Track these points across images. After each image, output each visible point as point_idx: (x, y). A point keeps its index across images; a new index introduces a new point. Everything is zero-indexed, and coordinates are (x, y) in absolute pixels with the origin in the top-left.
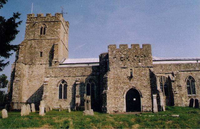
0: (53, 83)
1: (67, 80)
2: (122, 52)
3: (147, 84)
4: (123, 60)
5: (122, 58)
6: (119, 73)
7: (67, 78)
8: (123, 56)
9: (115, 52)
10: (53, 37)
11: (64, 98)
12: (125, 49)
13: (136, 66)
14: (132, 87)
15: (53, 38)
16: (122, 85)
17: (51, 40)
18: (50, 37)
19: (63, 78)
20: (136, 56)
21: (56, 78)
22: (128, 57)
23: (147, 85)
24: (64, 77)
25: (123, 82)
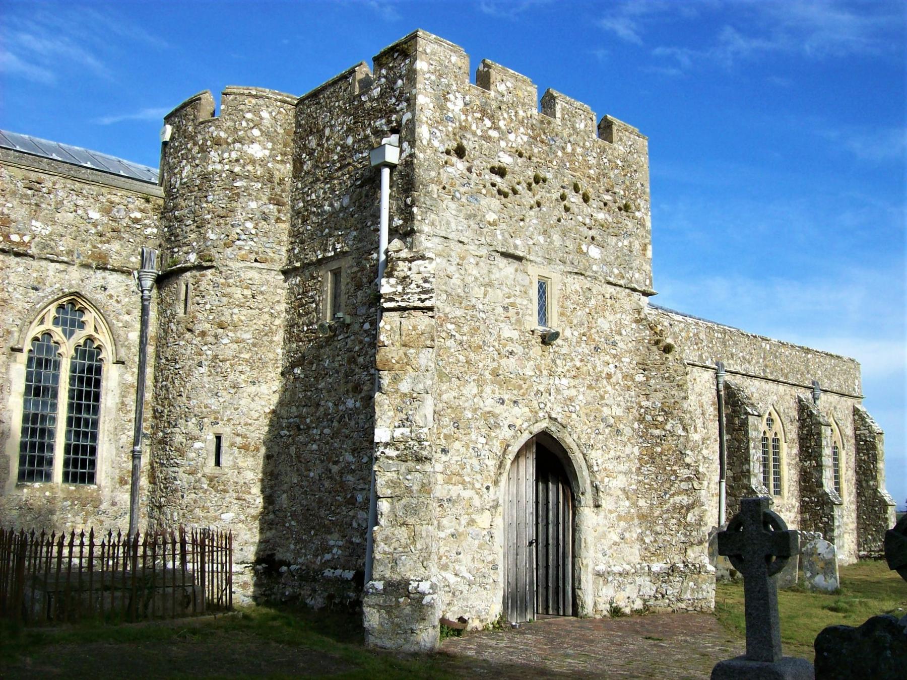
6: (478, 292)
8: (506, 160)
9: (460, 104)
16: (489, 404)
23: (618, 419)
25: (495, 373)
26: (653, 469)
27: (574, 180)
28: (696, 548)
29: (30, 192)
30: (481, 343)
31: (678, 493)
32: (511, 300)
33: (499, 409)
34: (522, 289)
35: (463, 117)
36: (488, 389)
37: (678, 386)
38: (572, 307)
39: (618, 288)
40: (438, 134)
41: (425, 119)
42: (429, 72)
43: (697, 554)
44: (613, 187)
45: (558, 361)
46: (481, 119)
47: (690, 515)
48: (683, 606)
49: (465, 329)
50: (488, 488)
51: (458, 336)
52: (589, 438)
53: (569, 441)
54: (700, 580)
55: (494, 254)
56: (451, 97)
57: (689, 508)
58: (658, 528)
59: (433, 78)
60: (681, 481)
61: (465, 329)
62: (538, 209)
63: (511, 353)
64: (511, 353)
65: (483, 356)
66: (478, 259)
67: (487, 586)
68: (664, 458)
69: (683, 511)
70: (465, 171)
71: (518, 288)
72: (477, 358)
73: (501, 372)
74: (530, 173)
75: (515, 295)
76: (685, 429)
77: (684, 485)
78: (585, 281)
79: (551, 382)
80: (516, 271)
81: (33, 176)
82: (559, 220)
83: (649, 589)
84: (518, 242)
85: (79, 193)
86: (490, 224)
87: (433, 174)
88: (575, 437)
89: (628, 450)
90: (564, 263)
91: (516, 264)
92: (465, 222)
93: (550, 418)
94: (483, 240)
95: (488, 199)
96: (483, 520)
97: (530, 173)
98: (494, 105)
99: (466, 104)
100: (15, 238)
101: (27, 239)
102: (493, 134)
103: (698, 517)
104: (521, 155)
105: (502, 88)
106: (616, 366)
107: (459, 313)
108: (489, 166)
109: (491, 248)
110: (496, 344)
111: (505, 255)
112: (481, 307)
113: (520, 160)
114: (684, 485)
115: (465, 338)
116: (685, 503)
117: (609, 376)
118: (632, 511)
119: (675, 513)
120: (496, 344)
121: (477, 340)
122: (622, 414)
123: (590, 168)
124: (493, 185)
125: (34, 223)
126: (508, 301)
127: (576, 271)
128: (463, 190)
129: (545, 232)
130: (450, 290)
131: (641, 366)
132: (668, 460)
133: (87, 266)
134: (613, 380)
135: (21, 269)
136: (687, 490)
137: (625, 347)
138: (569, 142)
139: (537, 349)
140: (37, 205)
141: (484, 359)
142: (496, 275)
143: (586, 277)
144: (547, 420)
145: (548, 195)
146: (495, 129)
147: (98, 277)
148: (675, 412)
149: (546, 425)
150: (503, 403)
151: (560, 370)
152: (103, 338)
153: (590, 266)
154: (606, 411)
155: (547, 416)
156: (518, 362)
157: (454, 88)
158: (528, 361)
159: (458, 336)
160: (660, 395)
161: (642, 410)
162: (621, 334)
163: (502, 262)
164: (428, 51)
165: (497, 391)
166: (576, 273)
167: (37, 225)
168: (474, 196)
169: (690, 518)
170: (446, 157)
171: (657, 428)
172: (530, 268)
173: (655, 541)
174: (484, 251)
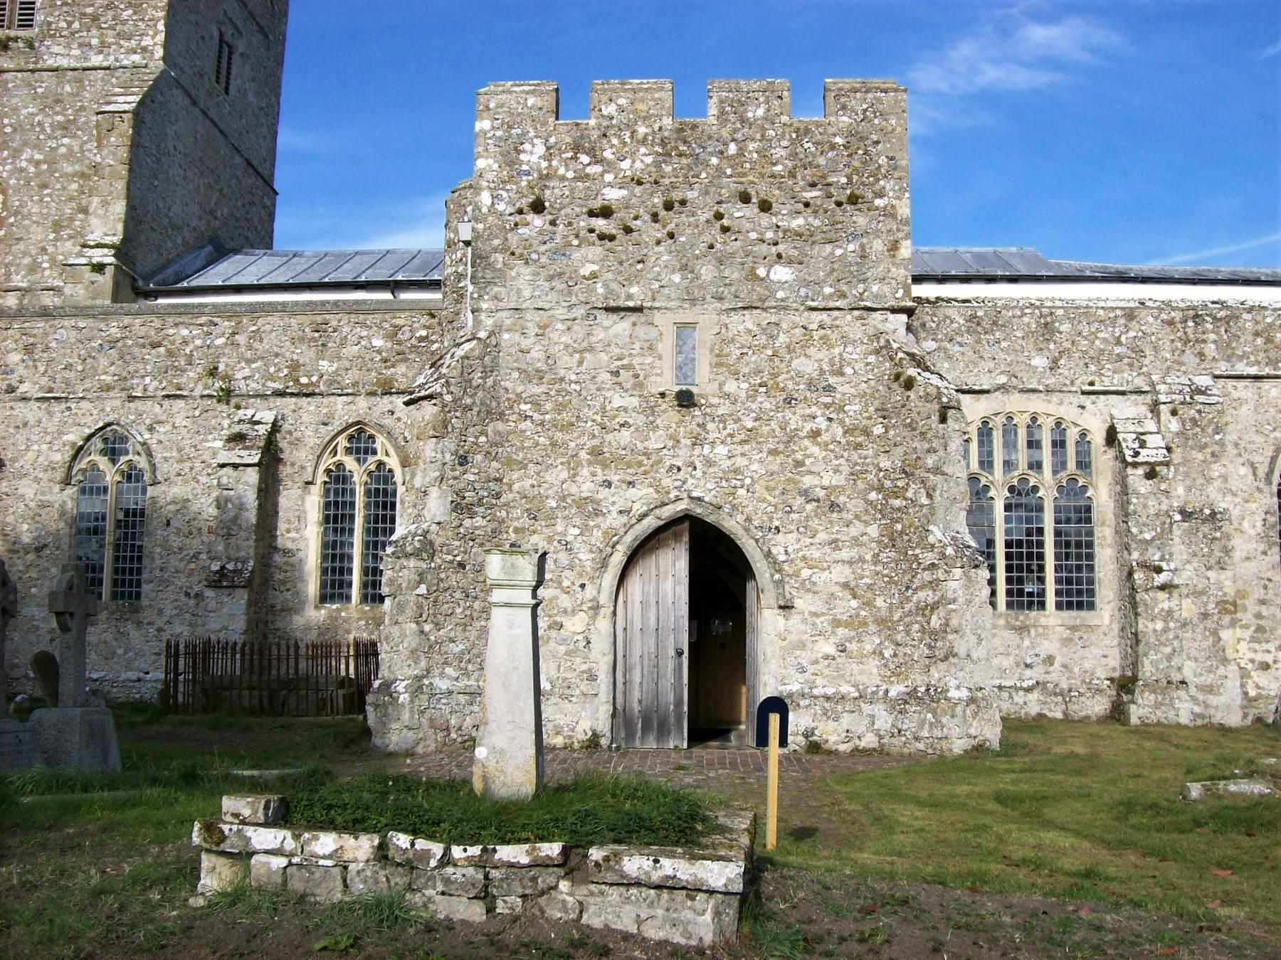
0: (31, 455)
1: (151, 429)
2: (608, 154)
3: (839, 480)
4: (612, 238)
5: (606, 212)
6: (568, 361)
7: (154, 409)
8: (613, 195)
9: (540, 149)
10: (103, 47)
11: (115, 596)
12: (642, 130)
13: (749, 293)
14: (681, 506)
15: (96, 60)
16: (586, 487)
17: (81, 81)
18: (76, 52)
19: (113, 409)
20: (745, 198)
21: (57, 408)
22: (668, 206)
24: (132, 398)
25: (596, 453)
26: (893, 554)
27: (741, 188)
28: (941, 666)
29: (317, 335)
30: (574, 419)
31: (922, 587)
32: (625, 362)
33: (603, 493)
34: (646, 345)
35: (544, 164)
36: (585, 472)
37: (922, 434)
38: (738, 352)
39: (836, 313)
40: (504, 194)
41: (485, 184)
42: (493, 128)
43: (942, 674)
44: (824, 177)
45: (710, 426)
46: (575, 158)
47: (934, 618)
48: (921, 746)
49: (548, 406)
50: (583, 586)
51: (536, 416)
52: (771, 519)
53: (731, 525)
54: (939, 711)
55: (595, 312)
56: (527, 147)
57: (934, 607)
58: (899, 638)
59: (499, 133)
60: (924, 570)
61: (548, 406)
62: (670, 241)
63: (622, 425)
64: (622, 425)
65: (575, 435)
66: (569, 323)
67: (574, 699)
68: (906, 538)
69: (927, 612)
70: (547, 226)
71: (637, 346)
72: (567, 437)
73: (605, 450)
74: (658, 200)
75: (630, 355)
76: (929, 496)
77: (927, 576)
78: (764, 314)
79: (696, 452)
80: (634, 324)
81: (319, 319)
82: (711, 247)
83: (884, 720)
84: (634, 290)
85: (363, 325)
86: (587, 279)
87: (496, 242)
88: (740, 518)
89: (854, 530)
90: (721, 299)
91: (634, 317)
92: (546, 284)
93: (691, 498)
94: (574, 300)
95: (583, 251)
96: (575, 624)
97: (656, 200)
98: (595, 134)
99: (548, 149)
100: (304, 380)
101: (314, 379)
102: (596, 169)
103: (943, 621)
104: (640, 183)
105: (610, 109)
106: (830, 419)
107: (537, 390)
108: (585, 210)
109: (589, 306)
110: (598, 418)
111: (607, 309)
112: (573, 377)
113: (638, 190)
114: (927, 576)
115: (548, 417)
116: (930, 601)
117: (815, 434)
118: (863, 613)
119: (917, 614)
120: (598, 418)
121: (566, 417)
122: (843, 483)
123: (775, 164)
124: (592, 231)
125: (321, 363)
126: (620, 363)
127: (740, 305)
128: (543, 248)
129: (684, 268)
130: (524, 366)
131: (880, 413)
132: (909, 541)
133: (372, 394)
134: (825, 437)
135: (312, 408)
136: (930, 582)
137: (853, 391)
138: (733, 140)
139: (669, 415)
140: (323, 345)
141: (579, 437)
142: (600, 335)
143: (765, 310)
144: (686, 501)
145: (691, 219)
146: (597, 162)
147: (385, 403)
148: (917, 472)
149: (684, 507)
150: (609, 485)
151: (711, 437)
152: (393, 462)
153: (772, 294)
154: (808, 481)
155: (685, 495)
156: (635, 435)
157: (532, 134)
158: (654, 431)
159: (536, 416)
160: (900, 450)
161: (881, 474)
162: (842, 374)
163: (606, 319)
164: (492, 105)
165: (599, 471)
166: (744, 308)
167: (324, 365)
168: (561, 252)
169: (935, 622)
170: (518, 218)
171: (897, 497)
172: (658, 318)
173: (895, 655)
174: (580, 312)
